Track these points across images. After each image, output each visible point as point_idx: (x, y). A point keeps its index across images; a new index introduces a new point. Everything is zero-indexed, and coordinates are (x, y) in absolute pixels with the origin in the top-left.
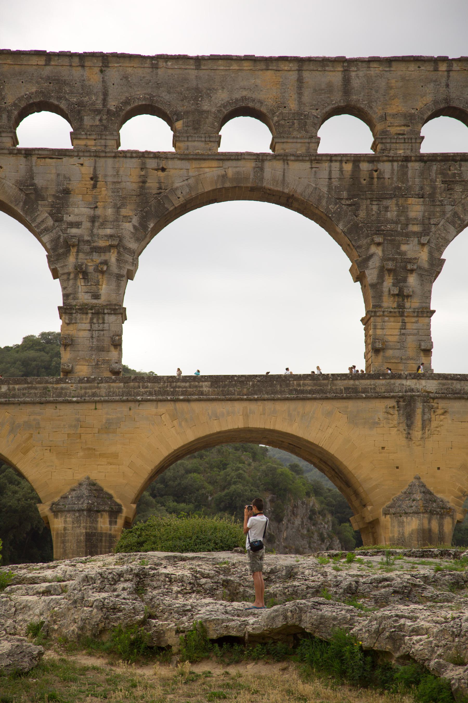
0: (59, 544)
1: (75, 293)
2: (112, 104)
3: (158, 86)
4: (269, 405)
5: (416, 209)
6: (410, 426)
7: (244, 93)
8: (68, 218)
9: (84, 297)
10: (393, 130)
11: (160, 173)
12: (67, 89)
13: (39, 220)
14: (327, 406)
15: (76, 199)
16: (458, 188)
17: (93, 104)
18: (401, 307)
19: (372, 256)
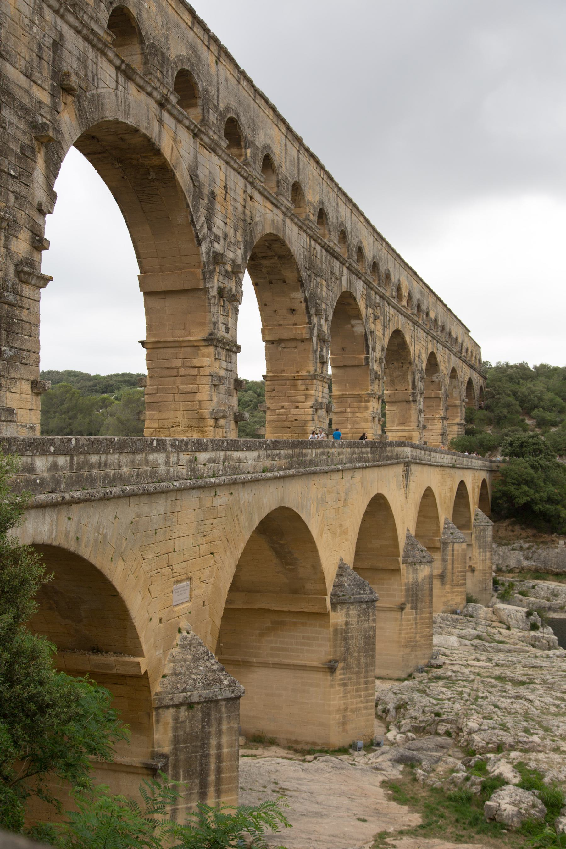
0: (339, 642)
5: (325, 289)
13: (200, 223)
15: (218, 207)
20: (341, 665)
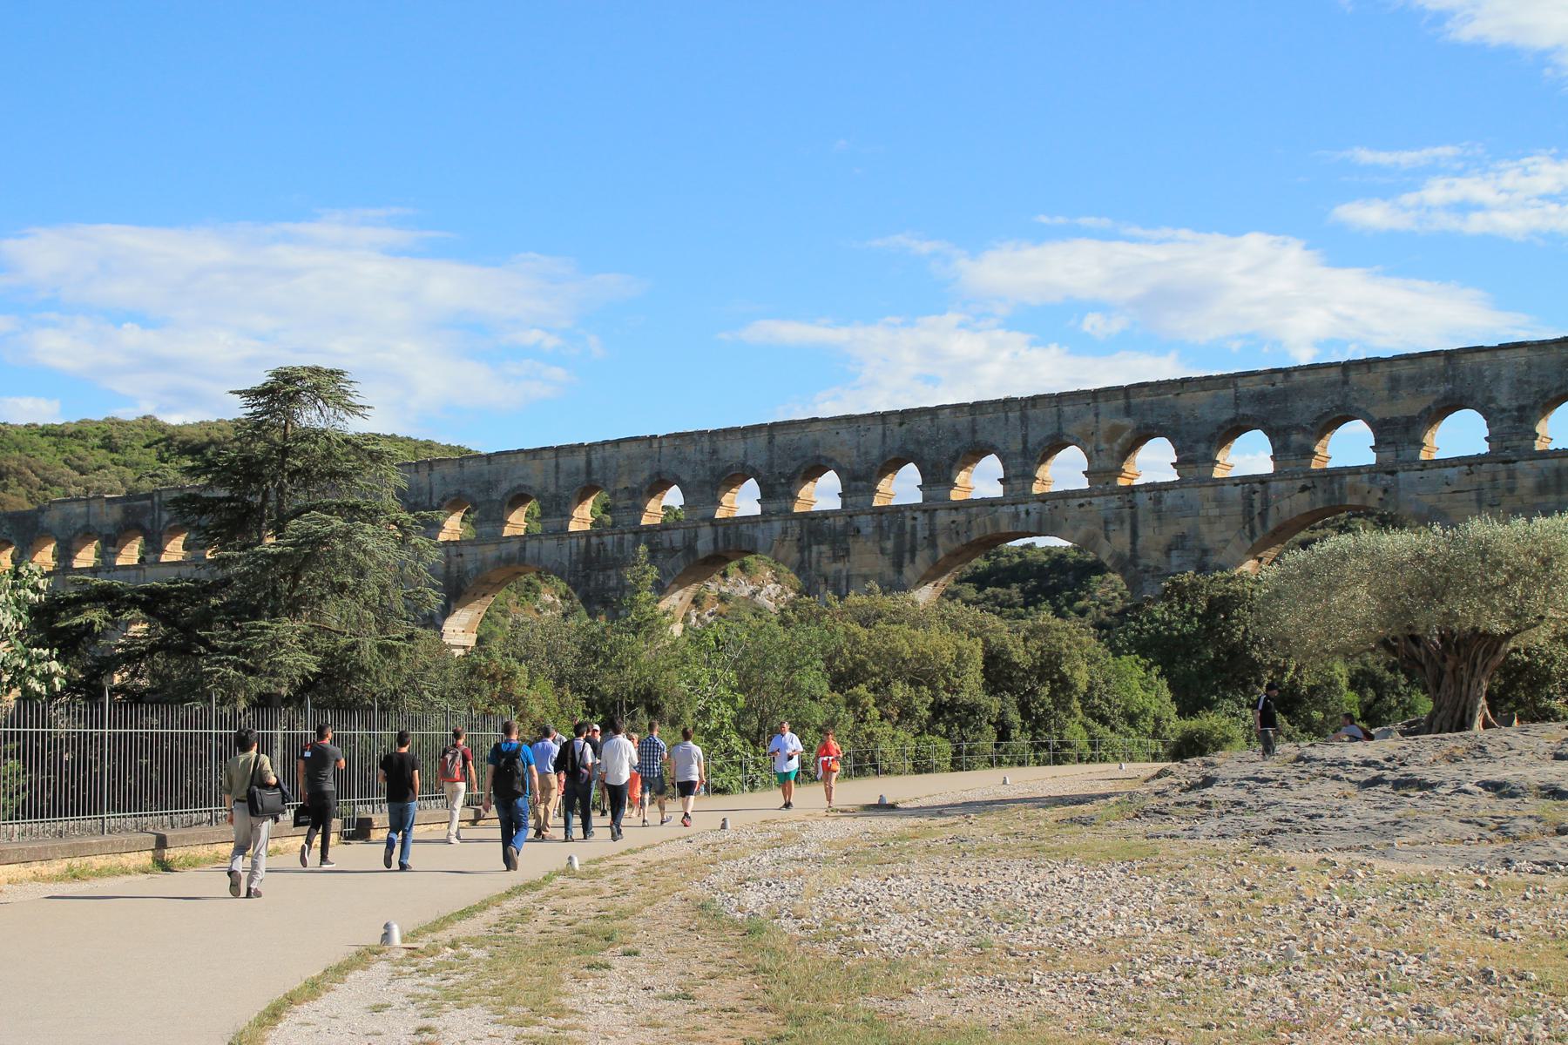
3: (464, 482)
7: (521, 482)
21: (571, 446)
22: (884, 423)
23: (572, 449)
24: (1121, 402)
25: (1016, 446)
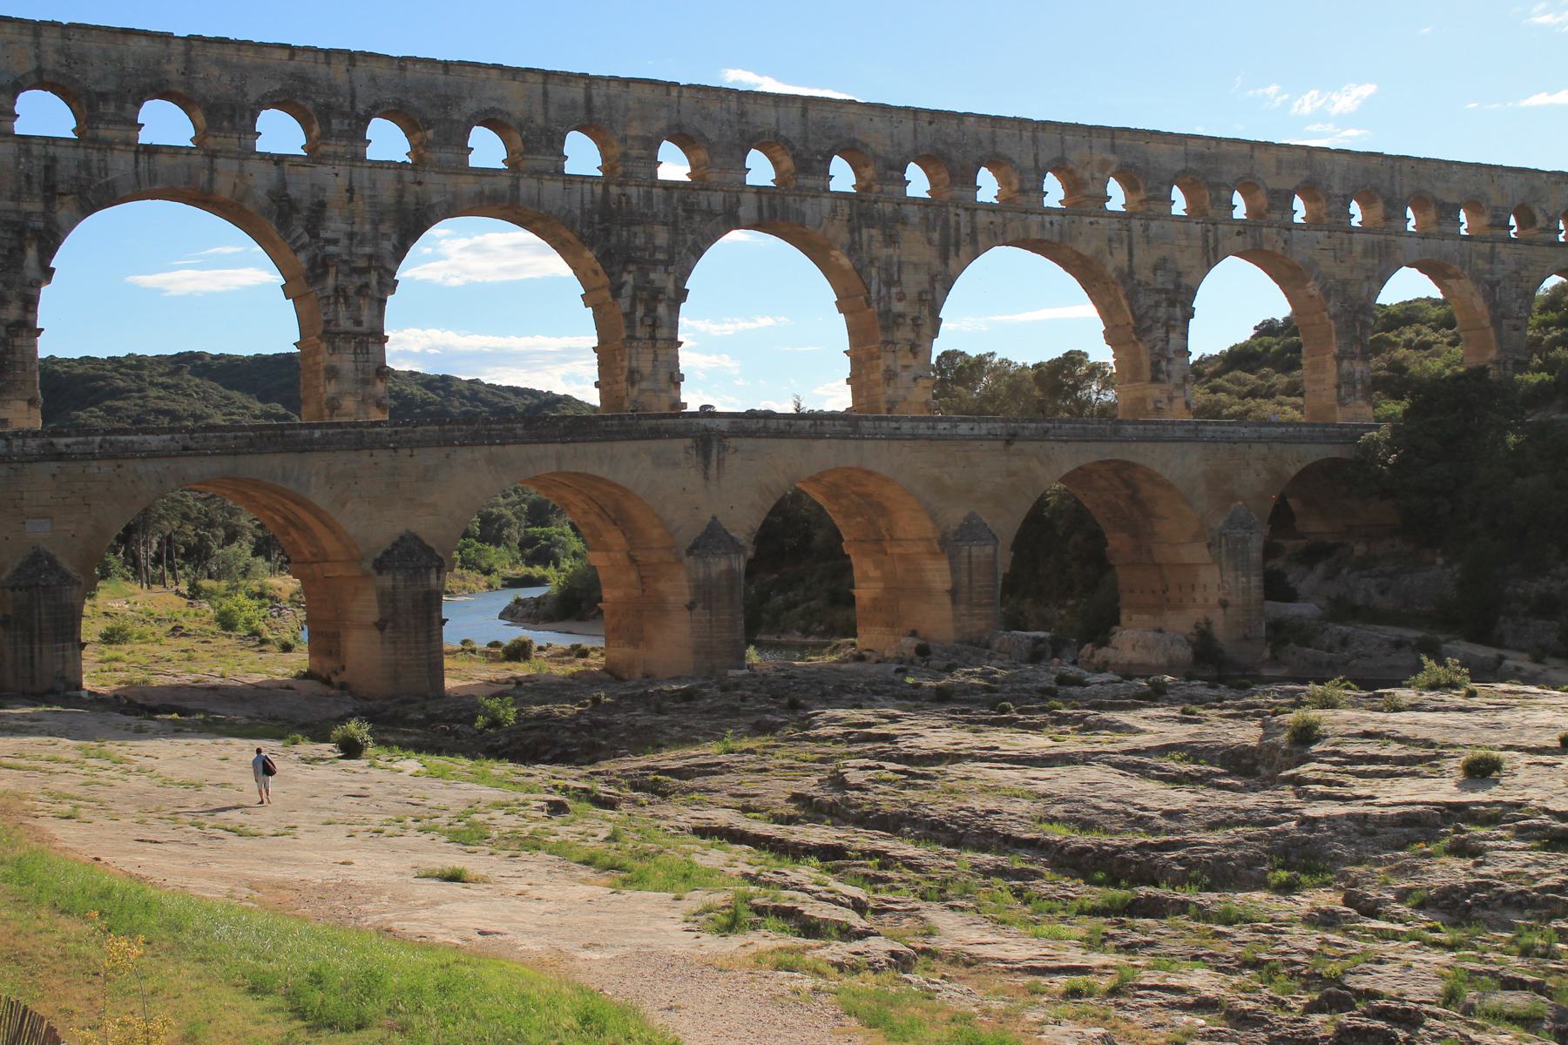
1: (337, 319)
2: (361, 108)
4: (580, 446)
5: (662, 237)
6: (707, 466)
7: (494, 104)
8: (323, 234)
9: (346, 324)
10: (634, 153)
11: (418, 188)
12: (313, 89)
13: (294, 235)
14: (633, 446)
16: (697, 218)
17: (341, 106)
18: (653, 338)
19: (624, 284)
20: (390, 625)
21: (569, 74)
22: (916, 119)
23: (567, 77)
24: (1108, 140)
25: (1029, 163)
